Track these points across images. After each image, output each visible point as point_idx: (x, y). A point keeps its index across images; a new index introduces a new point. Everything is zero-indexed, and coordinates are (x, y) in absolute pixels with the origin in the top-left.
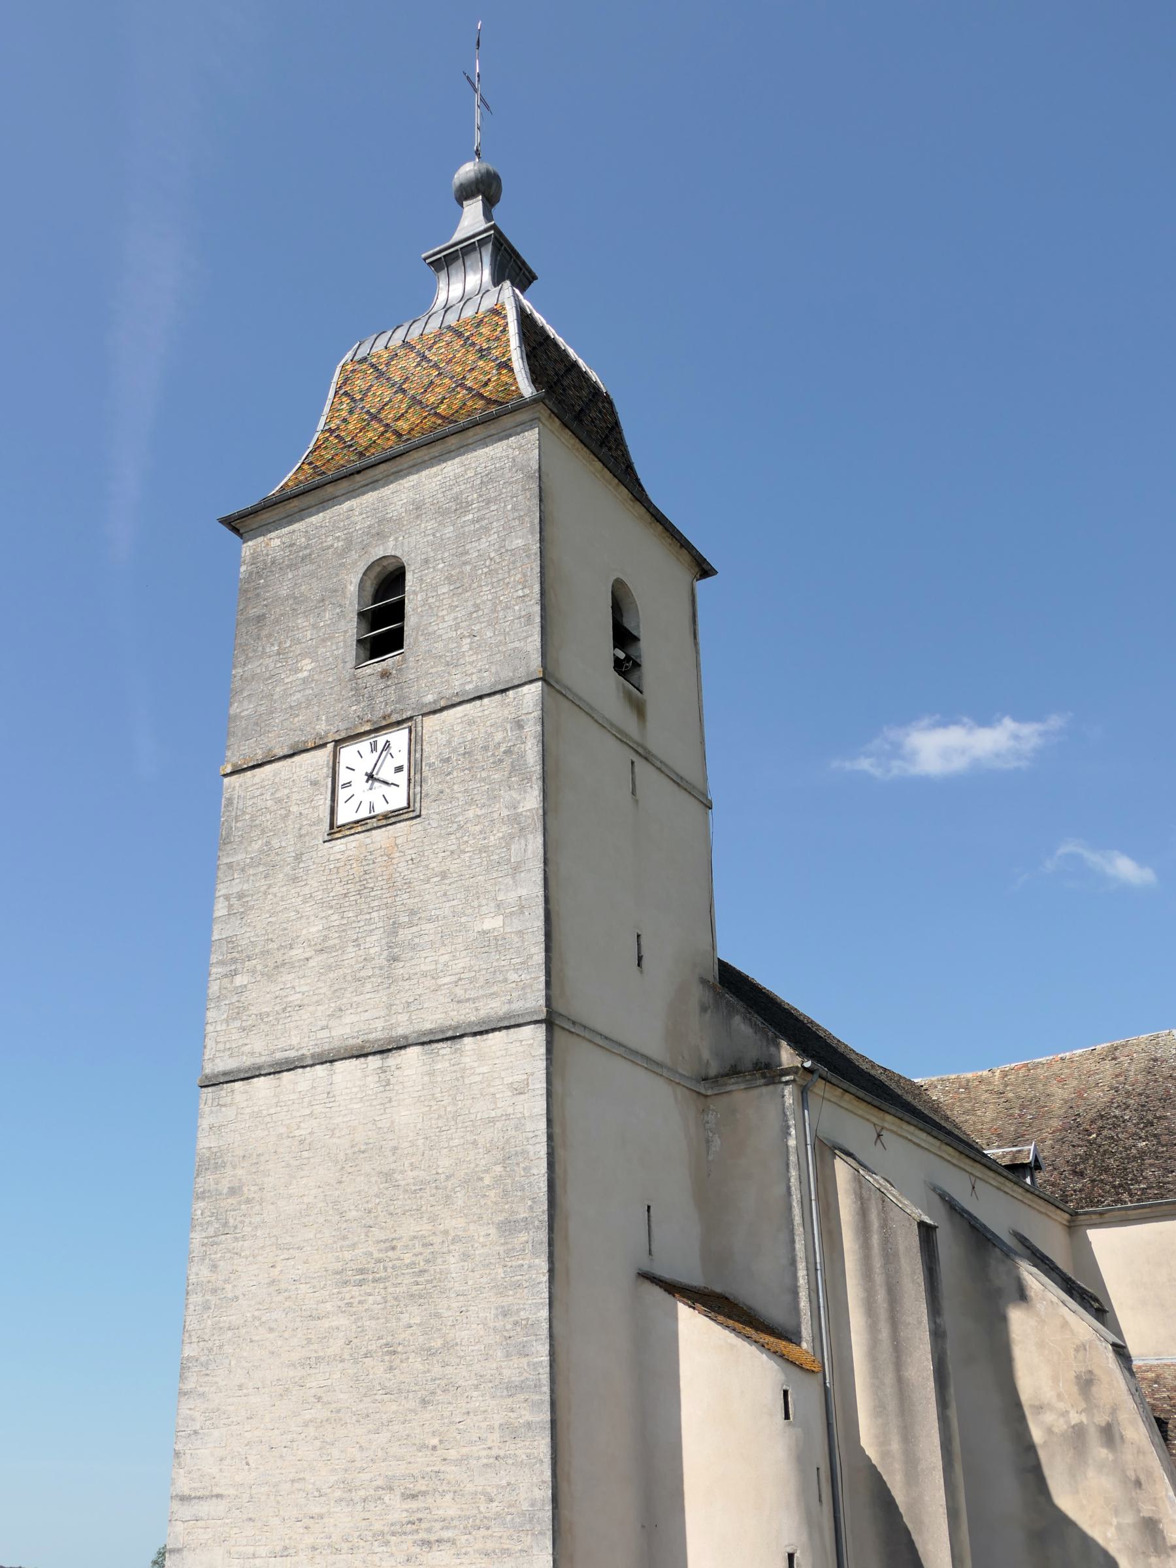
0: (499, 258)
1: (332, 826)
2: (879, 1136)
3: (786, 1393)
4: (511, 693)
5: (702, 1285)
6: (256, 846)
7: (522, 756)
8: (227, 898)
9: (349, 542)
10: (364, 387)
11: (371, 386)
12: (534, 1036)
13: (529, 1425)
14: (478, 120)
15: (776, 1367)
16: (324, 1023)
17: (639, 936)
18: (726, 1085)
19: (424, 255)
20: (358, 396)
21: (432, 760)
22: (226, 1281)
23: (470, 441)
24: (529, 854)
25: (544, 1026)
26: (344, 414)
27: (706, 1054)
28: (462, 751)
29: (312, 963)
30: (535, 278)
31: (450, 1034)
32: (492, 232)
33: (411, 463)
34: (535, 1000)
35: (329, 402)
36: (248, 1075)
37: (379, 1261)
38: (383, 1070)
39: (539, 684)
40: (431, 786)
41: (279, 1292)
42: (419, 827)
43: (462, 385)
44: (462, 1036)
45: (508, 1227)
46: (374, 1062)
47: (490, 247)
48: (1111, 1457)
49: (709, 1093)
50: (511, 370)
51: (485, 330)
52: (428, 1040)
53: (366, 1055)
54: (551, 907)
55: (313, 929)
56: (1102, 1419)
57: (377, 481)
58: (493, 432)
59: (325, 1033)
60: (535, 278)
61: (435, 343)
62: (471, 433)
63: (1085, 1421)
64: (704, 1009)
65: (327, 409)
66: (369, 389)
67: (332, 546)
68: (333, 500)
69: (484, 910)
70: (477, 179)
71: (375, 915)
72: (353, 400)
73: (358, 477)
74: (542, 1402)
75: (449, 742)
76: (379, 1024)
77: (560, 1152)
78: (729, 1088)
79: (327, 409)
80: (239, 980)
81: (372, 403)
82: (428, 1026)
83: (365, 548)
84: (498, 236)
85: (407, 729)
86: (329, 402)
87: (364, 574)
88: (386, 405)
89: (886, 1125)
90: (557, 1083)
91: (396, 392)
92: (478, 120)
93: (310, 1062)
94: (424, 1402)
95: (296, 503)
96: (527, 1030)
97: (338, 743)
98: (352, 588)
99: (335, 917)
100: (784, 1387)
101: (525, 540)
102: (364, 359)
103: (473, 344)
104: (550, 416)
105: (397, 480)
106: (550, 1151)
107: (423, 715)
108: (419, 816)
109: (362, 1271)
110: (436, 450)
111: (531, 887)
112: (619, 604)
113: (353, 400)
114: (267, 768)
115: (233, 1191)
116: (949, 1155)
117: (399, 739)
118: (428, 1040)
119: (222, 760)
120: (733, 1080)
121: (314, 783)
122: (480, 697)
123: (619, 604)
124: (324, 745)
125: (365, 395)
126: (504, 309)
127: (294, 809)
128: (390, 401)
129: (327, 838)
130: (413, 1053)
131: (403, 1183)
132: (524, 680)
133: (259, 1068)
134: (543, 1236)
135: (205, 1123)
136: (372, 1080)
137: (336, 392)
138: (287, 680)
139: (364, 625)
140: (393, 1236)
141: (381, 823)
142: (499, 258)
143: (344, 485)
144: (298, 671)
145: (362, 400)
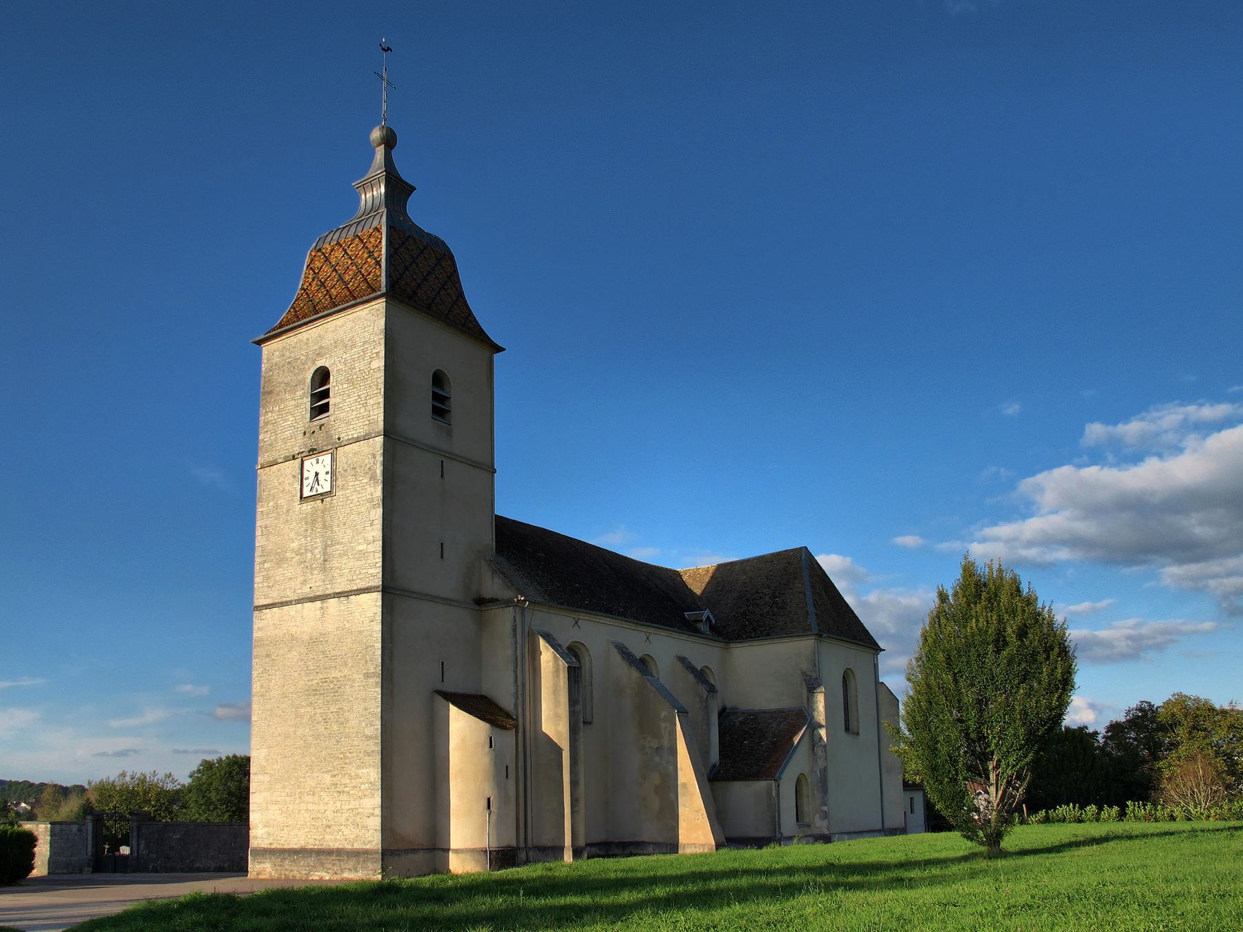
7: (375, 472)
8: (260, 526)
9: (307, 356)
10: (319, 265)
11: (322, 266)
12: (377, 596)
13: (373, 751)
14: (384, 97)
17: (442, 544)
19: (353, 184)
20: (317, 271)
21: (340, 470)
22: (267, 692)
24: (377, 517)
25: (380, 593)
26: (310, 280)
28: (352, 466)
29: (294, 560)
30: (412, 189)
32: (384, 173)
34: (378, 581)
35: (304, 273)
37: (321, 686)
38: (322, 608)
40: (339, 483)
41: (286, 697)
43: (360, 271)
45: (367, 676)
46: (318, 604)
50: (380, 267)
51: (372, 240)
52: (338, 595)
55: (295, 544)
60: (412, 189)
61: (351, 244)
65: (303, 276)
66: (321, 268)
67: (300, 358)
69: (360, 541)
71: (318, 540)
72: (315, 273)
74: (377, 743)
75: (347, 462)
79: (303, 276)
81: (322, 275)
83: (314, 361)
85: (330, 455)
86: (304, 273)
88: (328, 278)
91: (333, 271)
92: (384, 97)
94: (337, 741)
98: (309, 380)
99: (303, 540)
102: (320, 250)
103: (367, 248)
109: (315, 690)
112: (438, 379)
113: (315, 273)
115: (268, 656)
118: (338, 595)
119: (256, 462)
121: (294, 476)
123: (438, 379)
125: (320, 271)
126: (381, 228)
127: (287, 488)
128: (330, 276)
131: (329, 656)
135: (255, 627)
136: (318, 613)
137: (307, 268)
139: (314, 399)
140: (326, 677)
145: (318, 273)
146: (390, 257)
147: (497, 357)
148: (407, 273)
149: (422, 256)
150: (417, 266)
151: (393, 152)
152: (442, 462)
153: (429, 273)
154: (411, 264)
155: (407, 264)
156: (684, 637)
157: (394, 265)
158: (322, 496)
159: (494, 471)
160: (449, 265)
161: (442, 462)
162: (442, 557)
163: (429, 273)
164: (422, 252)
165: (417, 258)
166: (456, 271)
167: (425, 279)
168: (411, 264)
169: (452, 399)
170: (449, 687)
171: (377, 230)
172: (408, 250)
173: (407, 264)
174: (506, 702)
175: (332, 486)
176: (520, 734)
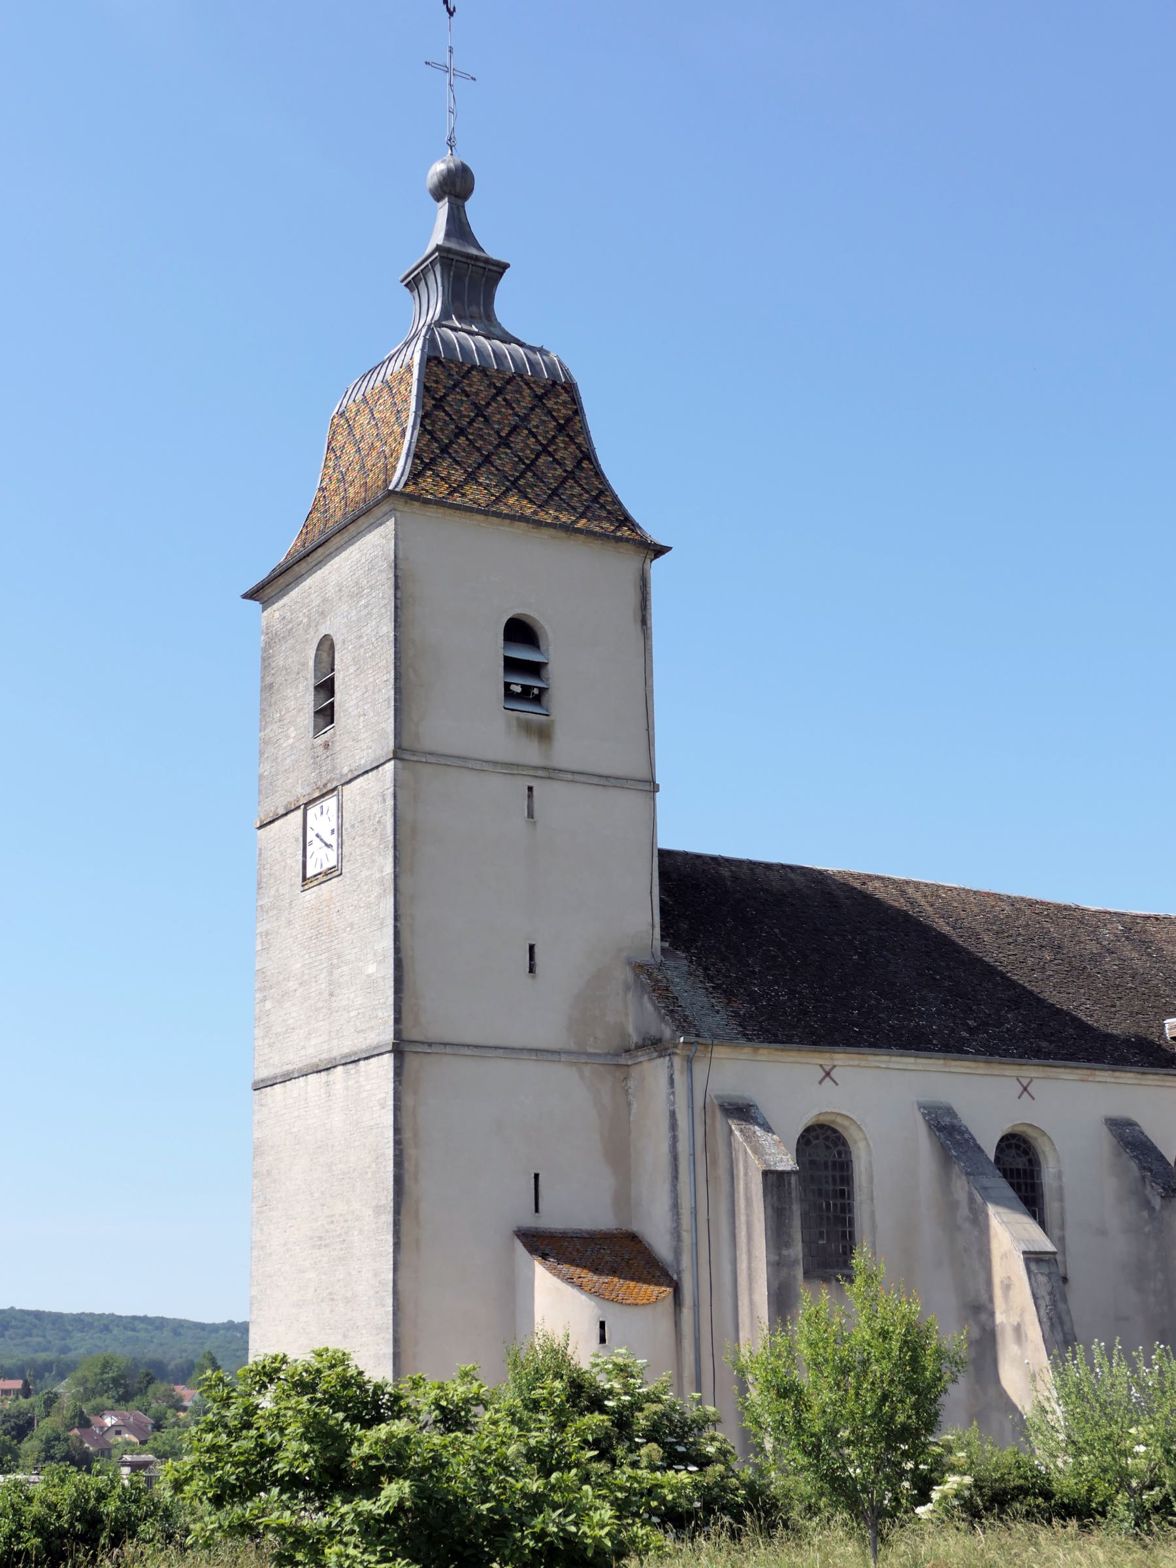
0: (452, 274)
1: (304, 878)
2: (828, 1074)
3: (602, 1325)
4: (380, 769)
5: (614, 1227)
6: (273, 892)
12: (388, 1060)
15: (593, 1303)
16: (302, 1044)
18: (637, 1057)
23: (362, 528)
25: (392, 1055)
27: (631, 1029)
31: (353, 1058)
32: (437, 254)
33: (335, 547)
36: (287, 1078)
38: (327, 1084)
39: (392, 762)
42: (341, 884)
44: (359, 1060)
45: (377, 1210)
47: (438, 268)
48: (1019, 1352)
49: (630, 1063)
53: (320, 1071)
54: (402, 955)
56: (1015, 1320)
57: (321, 562)
58: (372, 521)
59: (303, 1052)
62: (361, 521)
63: (1005, 1322)
64: (627, 988)
68: (299, 579)
70: (440, 183)
73: (309, 559)
76: (325, 1046)
77: (410, 1152)
78: (641, 1059)
80: (268, 1005)
82: (346, 1051)
84: (445, 255)
87: (318, 649)
89: (836, 1063)
90: (408, 1100)
93: (296, 1075)
95: (282, 581)
96: (387, 1055)
97: (306, 804)
100: (601, 1319)
101: (388, 629)
104: (406, 502)
105: (311, 575)
106: (398, 1153)
107: (343, 785)
108: (341, 874)
110: (346, 535)
111: (387, 943)
114: (276, 823)
116: (968, 1067)
117: (331, 803)
120: (640, 1053)
122: (367, 772)
124: (299, 807)
129: (302, 889)
130: (340, 1068)
132: (385, 759)
133: (276, 1078)
134: (389, 1218)
138: (284, 745)
141: (325, 878)
142: (452, 274)
143: (303, 566)
144: (288, 737)
146: (423, 417)
147: (658, 568)
148: (462, 440)
149: (499, 399)
150: (486, 420)
151: (471, 207)
152: (530, 789)
153: (514, 429)
154: (470, 423)
155: (464, 422)
156: (1104, 1076)
157: (430, 432)
158: (330, 874)
159: (655, 788)
160: (565, 403)
161: (530, 789)
162: (532, 970)
163: (514, 429)
164: (500, 391)
165: (488, 404)
166: (578, 411)
167: (505, 442)
168: (470, 423)
169: (550, 666)
170: (555, 1218)
171: (409, 369)
172: (467, 396)
173: (464, 422)
174: (661, 1244)
175: (341, 858)
176: (687, 1313)
